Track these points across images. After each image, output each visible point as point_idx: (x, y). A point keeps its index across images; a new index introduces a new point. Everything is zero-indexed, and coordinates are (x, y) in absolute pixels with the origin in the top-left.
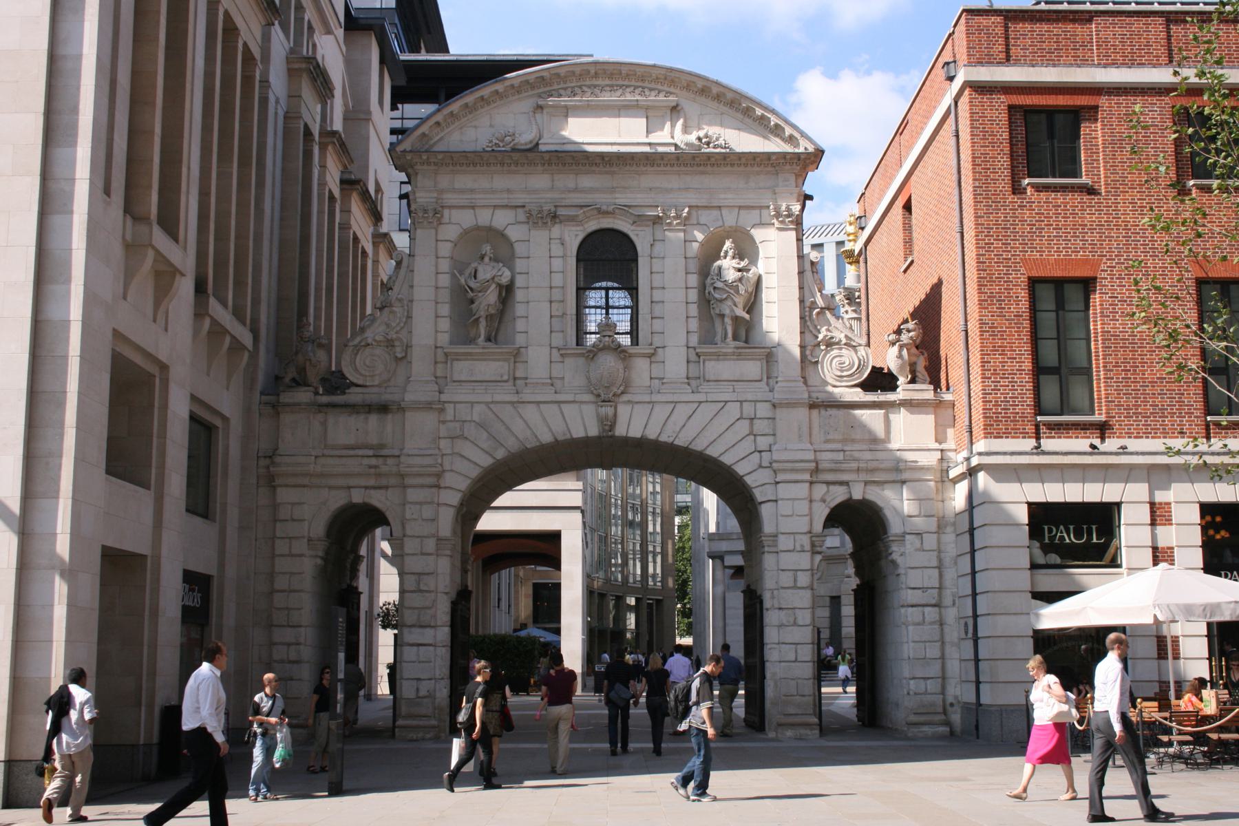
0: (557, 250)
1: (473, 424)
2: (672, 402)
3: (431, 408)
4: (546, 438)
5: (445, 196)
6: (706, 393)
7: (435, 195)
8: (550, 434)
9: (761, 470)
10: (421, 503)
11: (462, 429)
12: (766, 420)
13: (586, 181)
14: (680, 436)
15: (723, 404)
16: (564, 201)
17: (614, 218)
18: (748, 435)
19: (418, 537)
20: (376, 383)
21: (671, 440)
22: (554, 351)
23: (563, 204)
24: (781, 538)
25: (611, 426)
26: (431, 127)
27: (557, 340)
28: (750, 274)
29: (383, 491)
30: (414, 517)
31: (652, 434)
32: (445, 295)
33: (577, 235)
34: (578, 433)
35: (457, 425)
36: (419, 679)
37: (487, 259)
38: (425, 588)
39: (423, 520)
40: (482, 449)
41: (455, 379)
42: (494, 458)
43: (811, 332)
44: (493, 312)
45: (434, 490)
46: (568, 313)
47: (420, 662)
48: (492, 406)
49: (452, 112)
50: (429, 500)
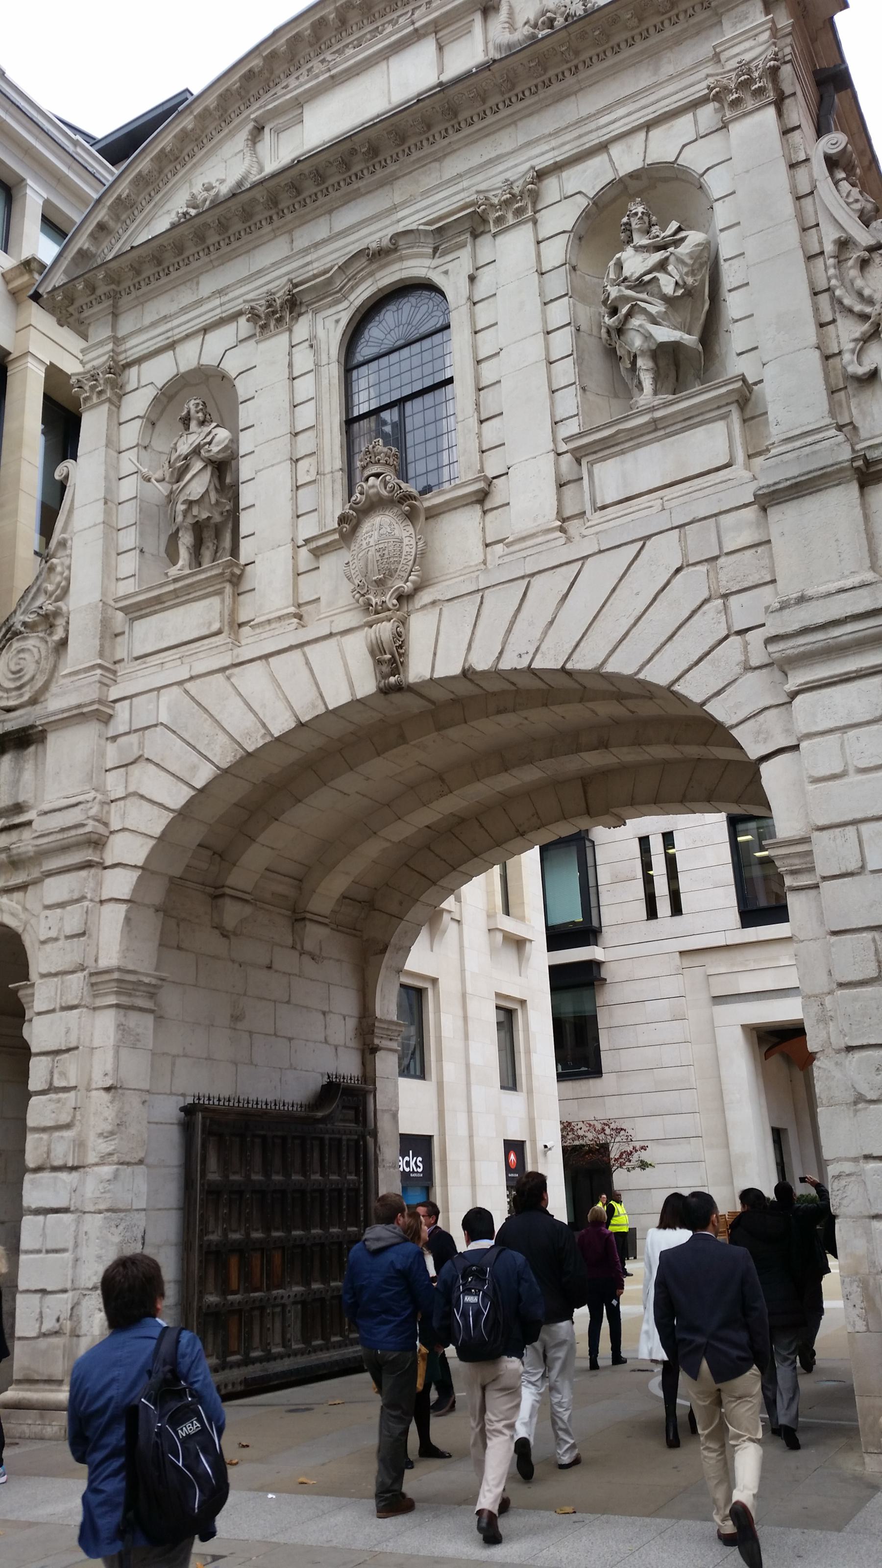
0: (303, 360)
1: (159, 729)
2: (523, 577)
3: (83, 714)
4: (281, 724)
5: (128, 345)
6: (597, 533)
7: (110, 346)
8: (288, 714)
9: (750, 675)
10: (62, 905)
11: (141, 745)
12: (749, 553)
13: (346, 217)
14: (543, 648)
15: (641, 543)
16: (310, 267)
17: (401, 259)
18: (706, 601)
19: (56, 975)
20: (26, 698)
21: (523, 663)
22: (304, 552)
23: (311, 273)
24: (822, 843)
25: (393, 660)
26: (92, 235)
27: (308, 528)
28: (683, 250)
29: (18, 895)
30: (53, 934)
31: (482, 662)
32: (128, 514)
33: (337, 321)
34: (338, 697)
35: (134, 738)
36: (44, 1292)
37: (193, 425)
38: (64, 1084)
39: (67, 937)
40: (173, 775)
41: (135, 655)
42: (193, 788)
43: (850, 311)
44: (204, 515)
45: (83, 873)
46: (328, 469)
47: (48, 1252)
48: (188, 686)
49: (120, 196)
50: (76, 896)
